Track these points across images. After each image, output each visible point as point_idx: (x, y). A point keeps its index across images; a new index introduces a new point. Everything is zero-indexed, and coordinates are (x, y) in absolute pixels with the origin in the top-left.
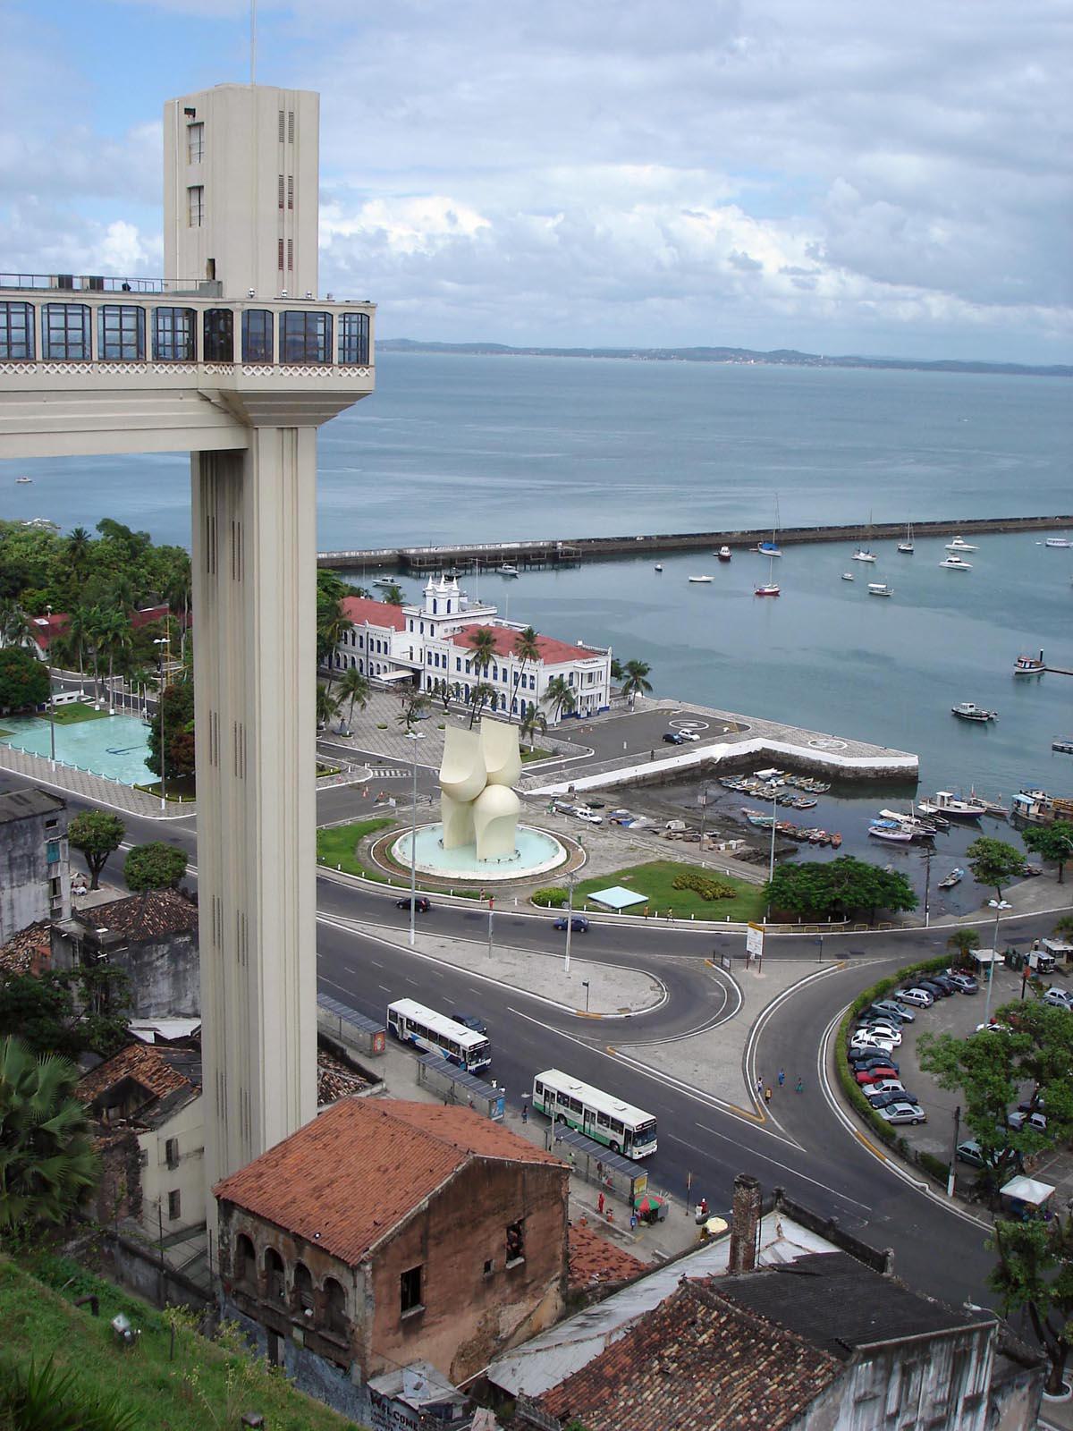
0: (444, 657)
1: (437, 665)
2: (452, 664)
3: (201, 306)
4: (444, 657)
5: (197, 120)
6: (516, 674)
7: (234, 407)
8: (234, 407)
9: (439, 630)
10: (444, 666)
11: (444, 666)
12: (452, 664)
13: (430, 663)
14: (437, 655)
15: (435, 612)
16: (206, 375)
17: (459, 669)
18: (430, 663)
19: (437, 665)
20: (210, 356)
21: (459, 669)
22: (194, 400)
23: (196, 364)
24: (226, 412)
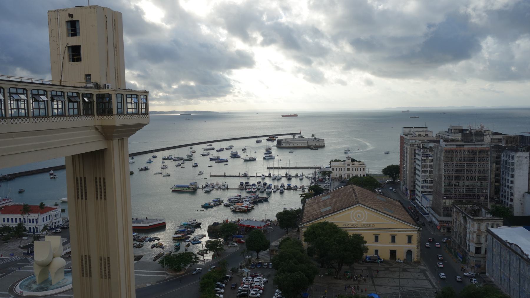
3: (95, 92)
5: (74, 19)
7: (107, 133)
8: (107, 133)
16: (97, 120)
20: (99, 114)
22: (94, 130)
23: (94, 115)
24: (102, 134)
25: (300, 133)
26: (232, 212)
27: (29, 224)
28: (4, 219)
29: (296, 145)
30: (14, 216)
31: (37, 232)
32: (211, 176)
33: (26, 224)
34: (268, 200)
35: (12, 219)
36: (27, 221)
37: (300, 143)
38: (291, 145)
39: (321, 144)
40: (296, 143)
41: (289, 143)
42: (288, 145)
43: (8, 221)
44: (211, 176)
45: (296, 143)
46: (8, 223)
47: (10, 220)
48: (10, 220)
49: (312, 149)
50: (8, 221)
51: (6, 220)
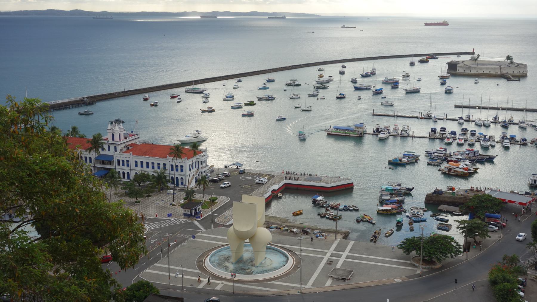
0: (128, 161)
1: (123, 165)
2: (132, 164)
4: (128, 161)
6: (172, 166)
9: (119, 148)
10: (128, 165)
11: (128, 165)
12: (132, 164)
13: (119, 164)
14: (123, 161)
15: (113, 139)
17: (136, 166)
18: (119, 164)
19: (123, 165)
21: (136, 166)
25: (473, 53)
26: (443, 176)
27: (177, 173)
28: (136, 162)
29: (480, 72)
30: (156, 160)
31: (182, 183)
32: (374, 115)
33: (167, 171)
34: (495, 160)
35: (147, 163)
36: (168, 167)
37: (488, 69)
38: (474, 72)
39: (522, 71)
40: (481, 69)
41: (469, 68)
42: (468, 72)
43: (148, 167)
44: (374, 115)
45: (481, 69)
46: (147, 170)
47: (145, 165)
48: (145, 165)
49: (508, 79)
50: (148, 167)
51: (139, 164)
